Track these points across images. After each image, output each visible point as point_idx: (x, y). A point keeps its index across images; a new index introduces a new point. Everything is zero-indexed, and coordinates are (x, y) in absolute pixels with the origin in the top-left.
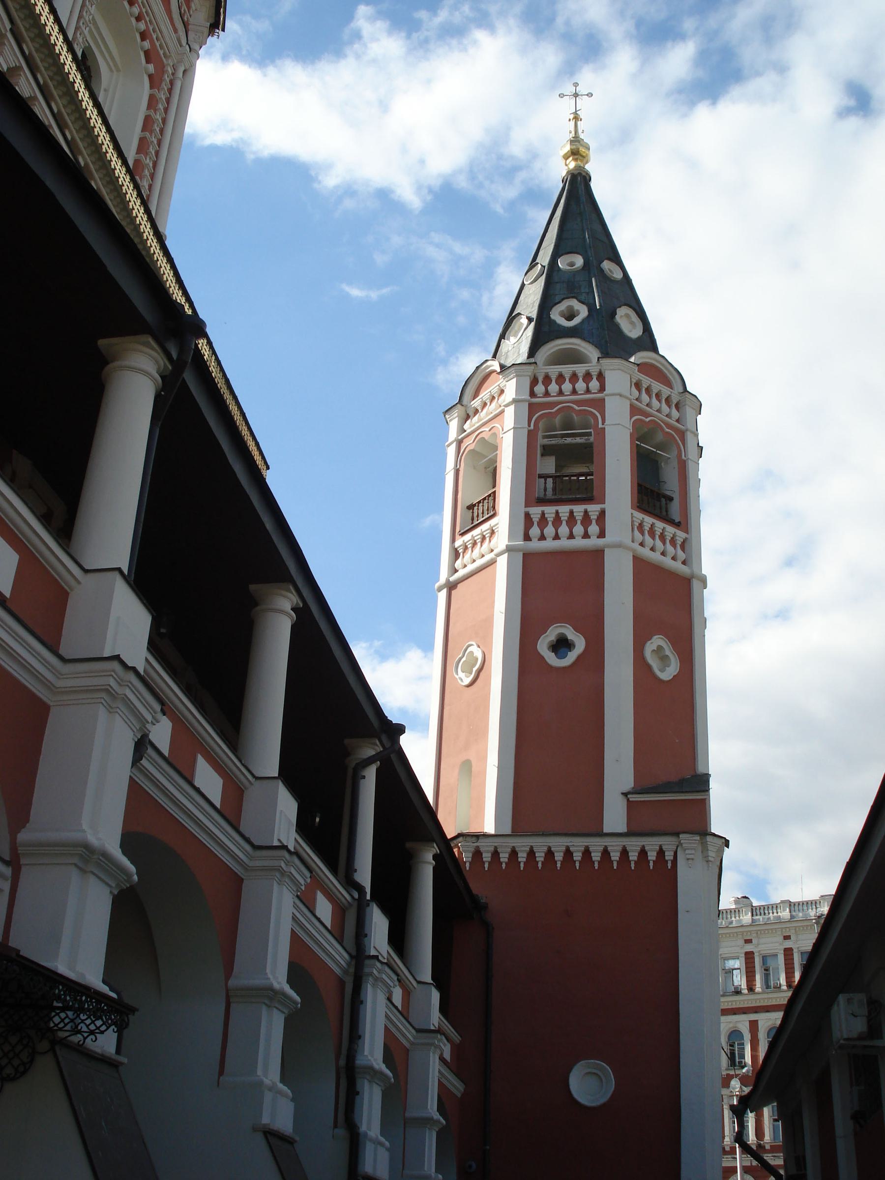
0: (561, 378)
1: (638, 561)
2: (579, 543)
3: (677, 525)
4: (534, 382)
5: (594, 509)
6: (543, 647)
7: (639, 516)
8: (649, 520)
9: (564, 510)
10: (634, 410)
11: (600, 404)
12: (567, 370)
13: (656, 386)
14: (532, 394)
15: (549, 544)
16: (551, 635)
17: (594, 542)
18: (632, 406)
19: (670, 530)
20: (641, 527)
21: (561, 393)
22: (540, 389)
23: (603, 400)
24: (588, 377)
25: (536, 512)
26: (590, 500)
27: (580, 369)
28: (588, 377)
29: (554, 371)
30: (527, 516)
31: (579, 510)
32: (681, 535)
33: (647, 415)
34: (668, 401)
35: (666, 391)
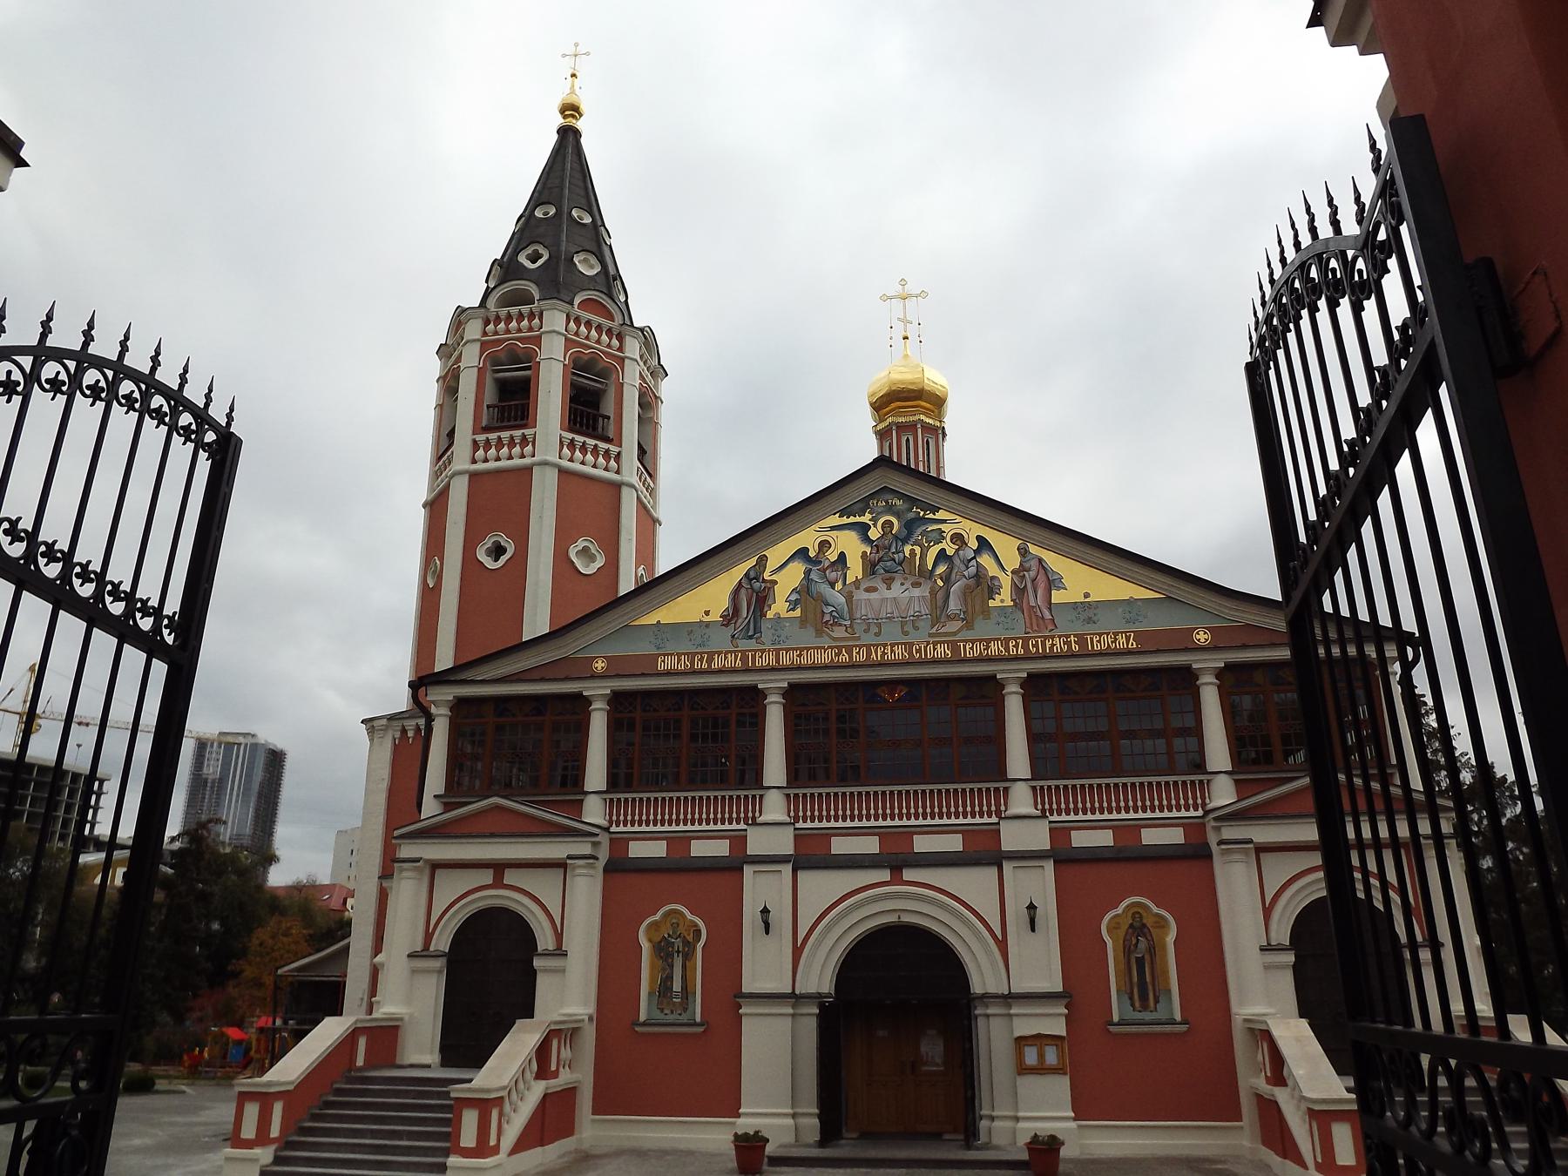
0: (509, 318)
2: (517, 462)
3: (608, 440)
4: (487, 323)
6: (482, 556)
7: (570, 435)
8: (580, 439)
9: (505, 435)
10: (569, 343)
11: (537, 340)
12: (514, 310)
14: (485, 334)
16: (489, 542)
17: (527, 461)
18: (567, 339)
19: (603, 445)
21: (508, 331)
22: (491, 327)
23: (540, 337)
25: (481, 438)
27: (525, 309)
28: (532, 316)
29: (503, 312)
30: (475, 442)
31: (518, 433)
32: (614, 449)
34: (609, 332)
35: (606, 323)
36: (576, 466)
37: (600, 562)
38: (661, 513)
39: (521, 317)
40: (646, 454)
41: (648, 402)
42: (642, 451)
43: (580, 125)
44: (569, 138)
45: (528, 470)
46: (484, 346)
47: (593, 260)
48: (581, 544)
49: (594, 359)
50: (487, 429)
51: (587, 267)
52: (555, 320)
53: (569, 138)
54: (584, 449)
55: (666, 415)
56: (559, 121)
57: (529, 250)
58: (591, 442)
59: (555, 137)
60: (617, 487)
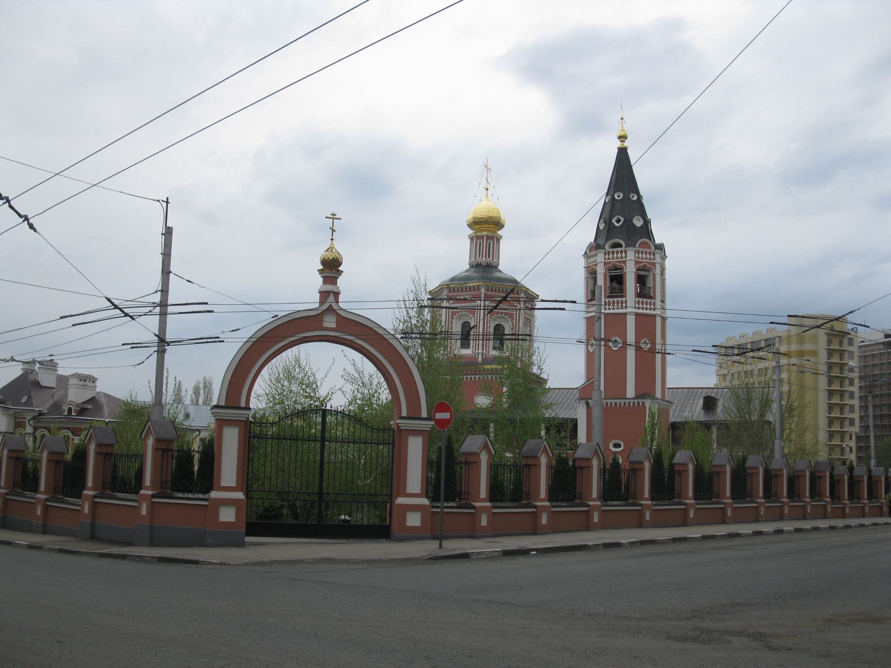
0: (613, 252)
2: (620, 311)
3: (651, 297)
5: (624, 299)
8: (641, 300)
9: (615, 300)
10: (636, 262)
11: (625, 262)
12: (615, 250)
15: (611, 311)
17: (624, 311)
19: (649, 301)
20: (638, 303)
24: (622, 252)
25: (607, 300)
26: (622, 296)
27: (619, 249)
28: (622, 252)
31: (620, 299)
32: (653, 301)
33: (641, 262)
34: (650, 253)
35: (648, 250)
36: (640, 311)
37: (649, 346)
39: (617, 252)
45: (625, 314)
46: (605, 264)
47: (640, 218)
49: (644, 266)
50: (609, 297)
51: (638, 222)
52: (631, 255)
54: (642, 304)
56: (618, 144)
57: (616, 218)
58: (645, 300)
59: (617, 151)
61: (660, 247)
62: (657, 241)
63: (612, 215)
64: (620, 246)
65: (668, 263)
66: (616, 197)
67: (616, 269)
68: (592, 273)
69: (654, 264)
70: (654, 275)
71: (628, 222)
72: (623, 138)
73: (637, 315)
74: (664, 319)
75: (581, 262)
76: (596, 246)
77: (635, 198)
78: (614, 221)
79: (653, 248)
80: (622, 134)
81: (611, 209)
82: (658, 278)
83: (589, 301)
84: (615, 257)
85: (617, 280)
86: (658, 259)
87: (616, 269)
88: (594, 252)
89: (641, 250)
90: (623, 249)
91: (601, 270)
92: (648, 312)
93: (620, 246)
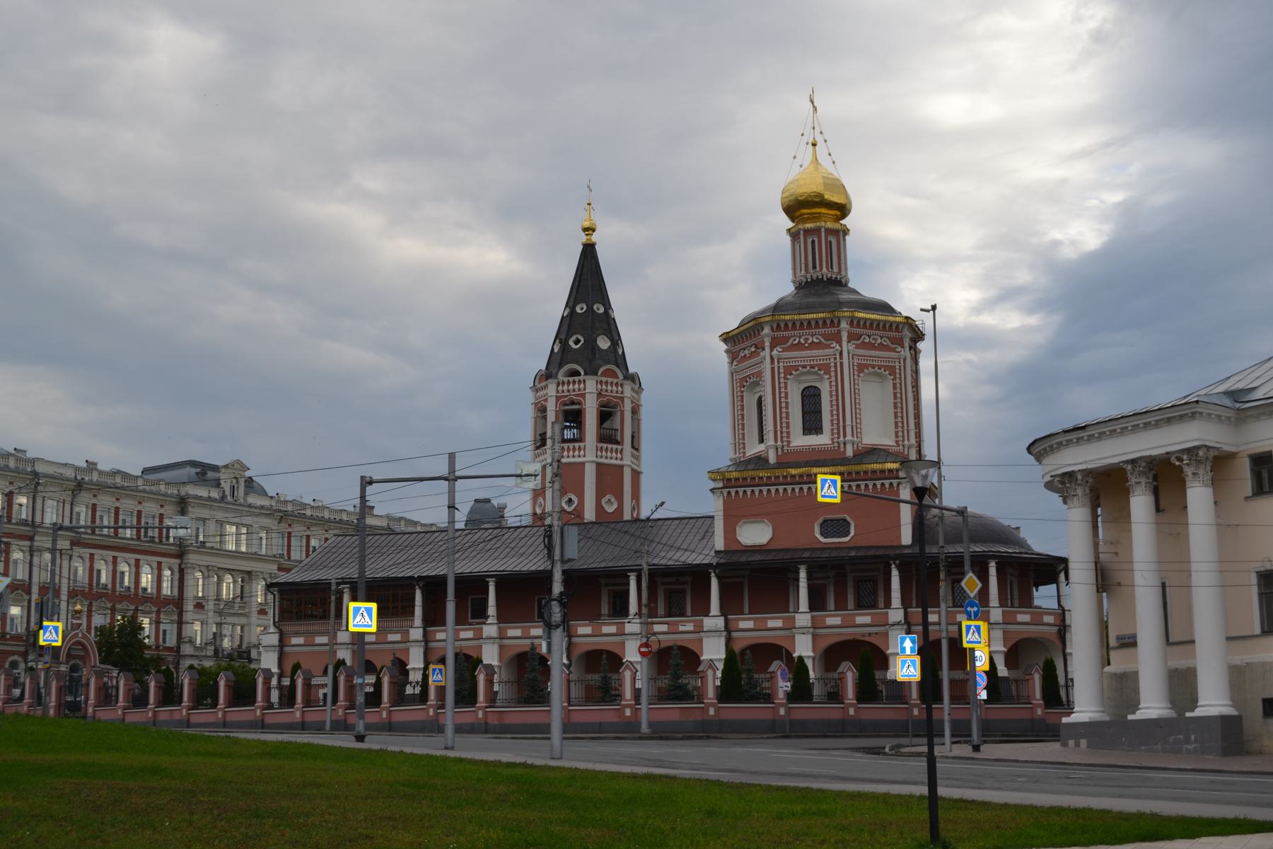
1: (599, 465)
2: (577, 460)
3: (617, 443)
4: (558, 384)
5: (582, 445)
8: (605, 445)
9: (571, 445)
10: (599, 394)
11: (583, 395)
12: (571, 379)
13: (610, 380)
17: (581, 460)
19: (615, 447)
27: (577, 379)
29: (566, 379)
32: (619, 447)
34: (617, 384)
35: (615, 381)
36: (603, 460)
37: (615, 506)
38: (643, 469)
39: (574, 382)
40: (635, 447)
41: (635, 411)
42: (633, 437)
43: (595, 238)
44: (589, 252)
45: (583, 464)
46: (558, 398)
48: (607, 497)
51: (603, 343)
52: (591, 385)
53: (589, 252)
54: (607, 450)
55: (644, 413)
56: (583, 238)
57: (574, 338)
58: (610, 446)
60: (622, 467)
61: (633, 378)
62: (631, 370)
63: (568, 337)
64: (578, 374)
65: (645, 399)
66: (578, 310)
67: (573, 403)
68: (541, 410)
69: (622, 399)
70: (622, 413)
71: (591, 345)
72: (589, 230)
73: (599, 465)
74: (636, 475)
75: (530, 397)
76: (547, 375)
77: (602, 310)
78: (571, 343)
79: (621, 377)
80: (587, 224)
81: (569, 324)
82: (628, 415)
83: (537, 448)
84: (572, 388)
85: (573, 417)
86: (628, 390)
87: (573, 403)
88: (543, 384)
89: (604, 379)
90: (581, 378)
91: (551, 407)
92: (613, 461)
93: (578, 374)
